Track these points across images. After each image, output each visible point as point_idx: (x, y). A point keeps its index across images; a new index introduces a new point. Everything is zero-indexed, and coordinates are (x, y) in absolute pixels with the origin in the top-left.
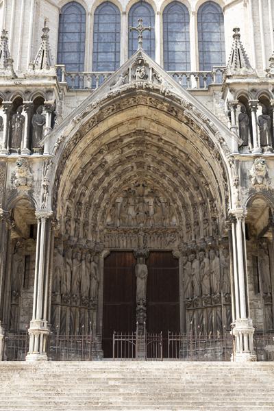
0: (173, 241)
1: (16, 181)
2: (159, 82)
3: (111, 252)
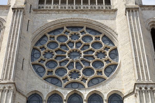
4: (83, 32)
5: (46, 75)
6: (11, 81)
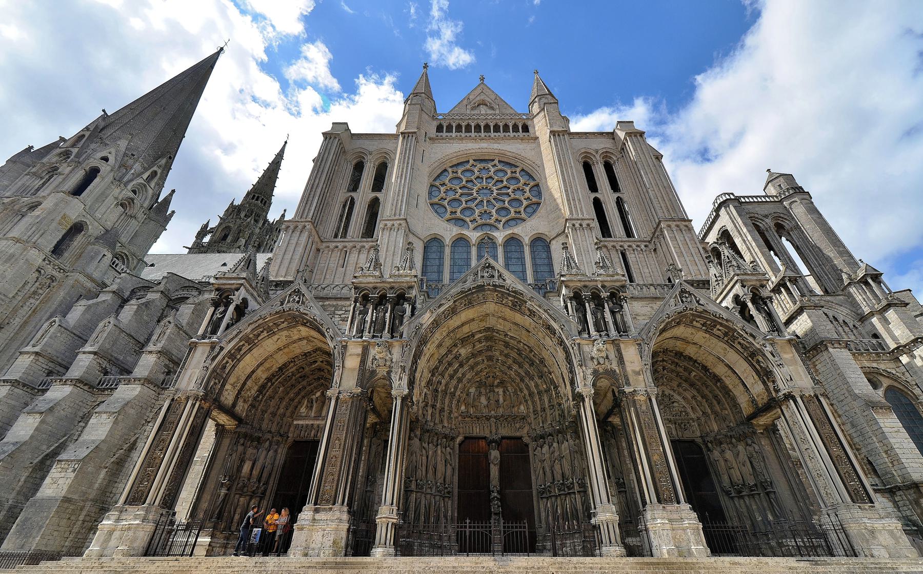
3: (466, 438)
4: (494, 166)
5: (448, 216)
6: (402, 217)
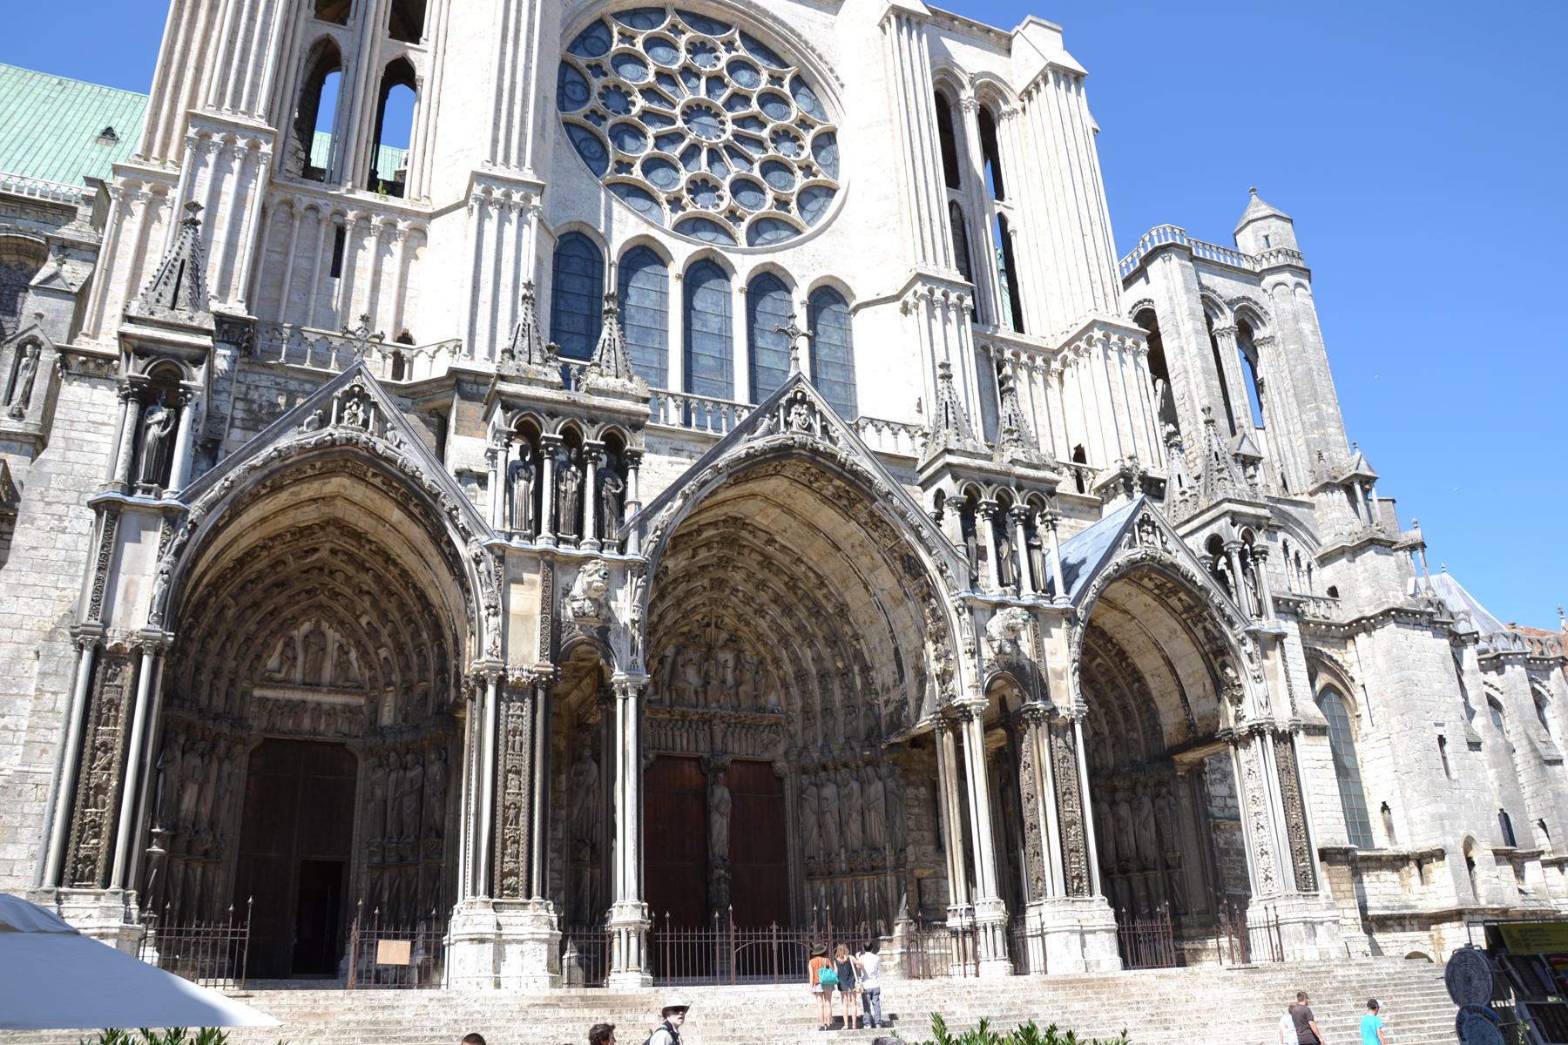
0: (774, 743)
1: (576, 605)
2: (831, 439)
3: (658, 757)
